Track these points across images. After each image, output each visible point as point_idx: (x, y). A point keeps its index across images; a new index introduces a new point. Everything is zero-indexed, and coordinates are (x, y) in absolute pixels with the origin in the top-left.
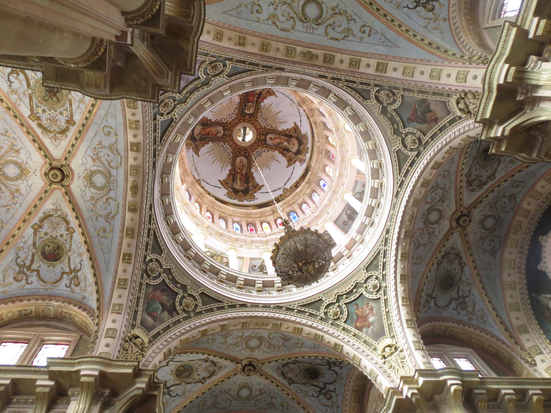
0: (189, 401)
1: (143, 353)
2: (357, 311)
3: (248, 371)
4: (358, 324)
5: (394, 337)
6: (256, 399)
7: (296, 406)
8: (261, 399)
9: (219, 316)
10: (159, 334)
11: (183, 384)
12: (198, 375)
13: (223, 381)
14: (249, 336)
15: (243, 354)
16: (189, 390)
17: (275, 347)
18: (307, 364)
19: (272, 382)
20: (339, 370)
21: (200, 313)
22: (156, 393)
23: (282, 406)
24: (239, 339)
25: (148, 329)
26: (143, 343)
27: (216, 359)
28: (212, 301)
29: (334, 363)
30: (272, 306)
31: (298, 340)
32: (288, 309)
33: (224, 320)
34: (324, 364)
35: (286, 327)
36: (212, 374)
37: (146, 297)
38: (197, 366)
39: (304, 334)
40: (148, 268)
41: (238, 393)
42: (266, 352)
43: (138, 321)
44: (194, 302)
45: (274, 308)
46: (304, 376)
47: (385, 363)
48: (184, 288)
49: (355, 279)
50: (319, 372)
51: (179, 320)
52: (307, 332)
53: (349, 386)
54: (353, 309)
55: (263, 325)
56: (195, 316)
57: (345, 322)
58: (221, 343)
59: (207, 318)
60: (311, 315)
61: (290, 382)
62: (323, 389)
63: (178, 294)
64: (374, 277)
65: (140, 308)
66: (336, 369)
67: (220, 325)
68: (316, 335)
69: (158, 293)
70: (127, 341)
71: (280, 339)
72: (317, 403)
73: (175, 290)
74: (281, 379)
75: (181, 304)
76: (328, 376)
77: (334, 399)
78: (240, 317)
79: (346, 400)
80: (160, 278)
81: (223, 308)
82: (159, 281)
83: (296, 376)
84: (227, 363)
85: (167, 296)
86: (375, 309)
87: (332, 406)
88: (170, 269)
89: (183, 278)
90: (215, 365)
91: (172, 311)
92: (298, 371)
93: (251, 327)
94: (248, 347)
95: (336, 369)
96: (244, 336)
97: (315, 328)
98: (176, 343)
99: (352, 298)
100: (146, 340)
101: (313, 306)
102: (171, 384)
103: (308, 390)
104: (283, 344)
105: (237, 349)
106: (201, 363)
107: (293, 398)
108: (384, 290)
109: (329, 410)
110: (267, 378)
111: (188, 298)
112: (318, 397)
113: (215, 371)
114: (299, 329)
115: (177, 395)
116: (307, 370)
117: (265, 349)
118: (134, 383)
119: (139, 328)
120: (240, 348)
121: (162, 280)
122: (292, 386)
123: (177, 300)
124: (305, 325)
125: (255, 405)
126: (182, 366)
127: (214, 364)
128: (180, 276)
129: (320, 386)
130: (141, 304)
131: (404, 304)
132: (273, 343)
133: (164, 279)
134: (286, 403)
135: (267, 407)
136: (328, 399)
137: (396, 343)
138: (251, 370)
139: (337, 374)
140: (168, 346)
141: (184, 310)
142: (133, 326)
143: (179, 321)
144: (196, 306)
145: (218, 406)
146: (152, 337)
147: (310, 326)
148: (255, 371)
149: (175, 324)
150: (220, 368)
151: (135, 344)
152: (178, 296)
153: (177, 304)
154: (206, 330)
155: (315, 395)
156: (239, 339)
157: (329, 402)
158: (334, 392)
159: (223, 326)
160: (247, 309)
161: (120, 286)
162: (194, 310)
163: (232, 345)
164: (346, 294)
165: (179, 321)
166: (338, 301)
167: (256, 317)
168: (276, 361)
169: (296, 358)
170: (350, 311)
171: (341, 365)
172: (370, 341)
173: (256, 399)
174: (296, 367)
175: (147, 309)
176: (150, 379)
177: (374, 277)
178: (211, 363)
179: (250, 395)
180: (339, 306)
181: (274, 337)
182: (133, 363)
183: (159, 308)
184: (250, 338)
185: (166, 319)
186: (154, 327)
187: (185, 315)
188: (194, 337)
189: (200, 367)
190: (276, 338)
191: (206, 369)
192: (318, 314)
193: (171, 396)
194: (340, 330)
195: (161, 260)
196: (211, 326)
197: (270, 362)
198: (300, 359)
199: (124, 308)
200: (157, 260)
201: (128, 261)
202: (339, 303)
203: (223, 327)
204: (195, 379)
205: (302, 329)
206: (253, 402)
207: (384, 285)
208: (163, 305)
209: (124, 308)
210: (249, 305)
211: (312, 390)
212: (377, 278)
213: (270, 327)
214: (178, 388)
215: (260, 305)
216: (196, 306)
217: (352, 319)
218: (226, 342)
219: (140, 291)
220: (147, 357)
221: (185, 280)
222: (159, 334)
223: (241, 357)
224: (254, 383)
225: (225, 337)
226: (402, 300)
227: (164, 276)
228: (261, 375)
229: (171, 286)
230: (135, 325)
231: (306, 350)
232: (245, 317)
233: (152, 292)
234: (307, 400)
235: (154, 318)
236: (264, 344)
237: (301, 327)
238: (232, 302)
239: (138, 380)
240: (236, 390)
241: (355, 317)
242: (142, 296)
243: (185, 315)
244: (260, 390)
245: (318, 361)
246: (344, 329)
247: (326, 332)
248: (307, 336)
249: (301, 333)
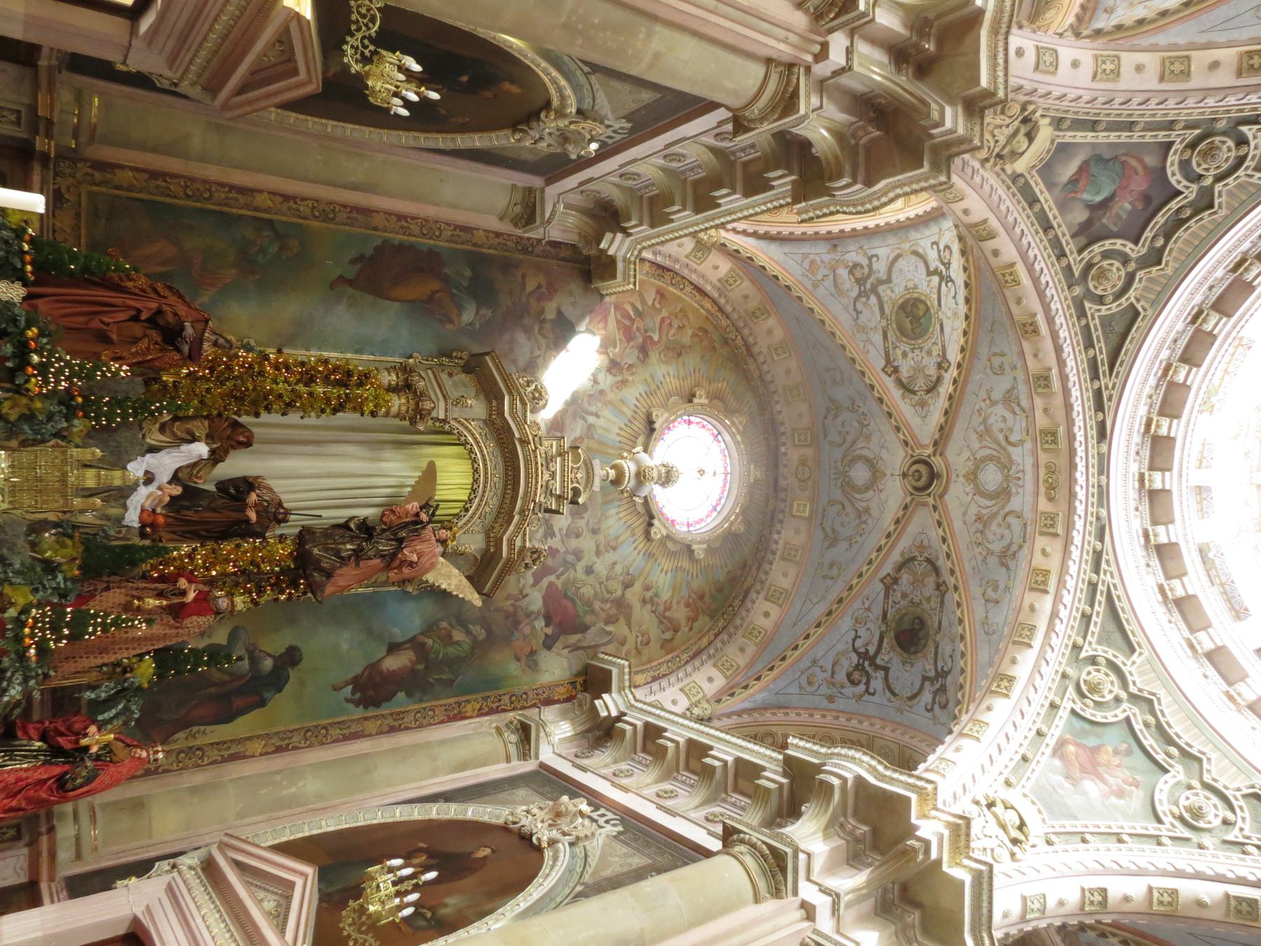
0: (845, 342)
1: (992, 160)
2: (1110, 749)
3: (917, 471)
4: (1071, 748)
5: (1049, 843)
6: (847, 504)
7: (833, 596)
8: (847, 515)
9: (1075, 364)
10: (1032, 201)
11: (884, 323)
12: (905, 355)
13: (890, 415)
14: (1011, 461)
15: (957, 457)
16: (869, 340)
17: (982, 532)
18: (936, 619)
19: (889, 536)
20: (922, 704)
21: (1082, 313)
22: (926, 167)
23: (831, 565)
24: (1001, 437)
25: (1047, 169)
26: (1016, 155)
27: (946, 388)
28: (1116, 340)
29: (943, 689)
30: (1103, 512)
31: (1007, 588)
32: (1098, 556)
33: (1064, 378)
34: (940, 665)
35: (1048, 549)
36: (907, 388)
37: (1132, 149)
38: (927, 346)
39: (1029, 598)
40: (1217, 139)
41: (860, 457)
42: (965, 514)
43: (1069, 137)
44: (1110, 291)
45: (1098, 518)
46: (905, 614)
47: (977, 803)
48: (1154, 257)
49: (1214, 756)
50: (915, 653)
51: (1064, 255)
52: (1037, 606)
53: (883, 728)
54: (1114, 739)
55: (1051, 487)
56: (1073, 298)
57: (1073, 712)
58: (989, 391)
59: (1067, 334)
60: (1086, 618)
61: (888, 580)
62: (873, 663)
63: (1136, 242)
64: (1230, 816)
65: (1102, 137)
66: (927, 697)
67: (1050, 369)
68: (1033, 628)
69: (1139, 184)
70: (1024, 109)
71: (1005, 543)
72: (841, 647)
73: (1148, 234)
74: (896, 557)
75: (1106, 255)
76: (906, 675)
77: (849, 690)
78: (1070, 422)
79: (849, 720)
80: (1185, 183)
81: (1095, 376)
82: (1175, 178)
83: (904, 596)
84: (936, 417)
85: (1130, 214)
86: (1122, 802)
87: (833, 684)
88: (1212, 206)
89: (1181, 251)
90: (928, 391)
91: (1088, 234)
92: (917, 600)
93: (1043, 458)
94: (979, 464)
95: (927, 697)
96: (1010, 449)
97: (1051, 627)
98: (1009, 252)
99: (1149, 741)
100: (1020, 166)
101: (1112, 627)
102: (882, 294)
103: (870, 625)
104: (990, 552)
105: (974, 436)
106: (935, 353)
107: (851, 588)
108: (1188, 840)
109: (824, 675)
110: (897, 522)
111: (1123, 273)
112: (855, 650)
113: (914, 392)
114: (1045, 583)
115: (858, 313)
116: (922, 622)
117: (973, 510)
118: (952, 103)
119: (1052, 142)
120: (976, 445)
121: (1180, 187)
122: (880, 587)
123: (1118, 244)
124: (1058, 599)
125: (831, 503)
126: (928, 309)
127: (932, 388)
128: (1187, 242)
129: (880, 656)
130: (1113, 137)
131: (1156, 894)
132: (994, 527)
133: (1180, 193)
134: (839, 575)
135: (829, 531)
136: (849, 676)
137: (1033, 846)
138: (919, 480)
139: (911, 698)
140: (1001, 230)
141: (1089, 266)
142: (1058, 123)
143: (1061, 255)
144: (1100, 300)
145: (831, 417)
146: (1027, 183)
147: (1054, 614)
148: (915, 488)
149: (1056, 244)
150: (923, 404)
151: (1016, 132)
152: (1130, 245)
153: (1107, 244)
154: (1036, 331)
155: (859, 643)
156: (1001, 437)
157: (841, 677)
158: (867, 691)
159: (1047, 378)
160: (1093, 442)
161: (1167, 64)
162: (1089, 295)
163: (985, 421)
164: (1159, 726)
165: (1061, 255)
166: (1134, 698)
167: (1073, 466)
168: (944, 540)
169: (956, 588)
170: (1107, 730)
171: (936, 707)
172: (1028, 773)
173: (847, 504)
174: (927, 594)
175: (1099, 159)
176: (961, 141)
177: (1230, 816)
178: (934, 379)
179: (854, 488)
180: (1117, 700)
181: (1009, 526)
182: (1001, 87)
183: (1098, 193)
184: (1005, 465)
185: (1069, 217)
186: (1050, 186)
188: (1019, 301)
189: (924, 354)
190: (1006, 532)
191: (919, 369)
192: (1089, 638)
193: (856, 300)
194: (1051, 696)
195: (1241, 172)
196: (1048, 343)
197: (939, 524)
198: (952, 597)
199: (1110, 86)
200: (1241, 160)
201: (1245, 65)
202: (1128, 701)
203: (1043, 380)
204: (894, 348)
205: (1046, 592)
206: (838, 495)
207: (1206, 840)
208: (1105, 204)
209: (1110, 86)
210: (1104, 448)
211: (869, 637)
212: (1225, 822)
213: (1044, 505)
214: (873, 313)
215: (1104, 478)
216: (1100, 300)
217: (1083, 733)
218: (994, 403)
219: (1150, 127)
220: (981, 171)
221: (1176, 259)
222: (1032, 201)
223: (950, 452)
224: (883, 496)
225: (1009, 398)
226: (1166, 890)
227: (1191, 192)
228: (906, 507)
229: (1160, 219)
230: (1060, 130)
231: (979, 612)
232: (1071, 437)
233: (1145, 167)
234: (846, 624)
235: (1074, 181)
236: (989, 503)
237: (1052, 587)
238: (1110, 399)
239: (960, 109)
240: (866, 453)
241: (1091, 742)
242: (1136, 137)
244: (867, 510)
245: (946, 648)
246: (1054, 706)
247: (1042, 656)
248: (1026, 604)
249: (1032, 589)
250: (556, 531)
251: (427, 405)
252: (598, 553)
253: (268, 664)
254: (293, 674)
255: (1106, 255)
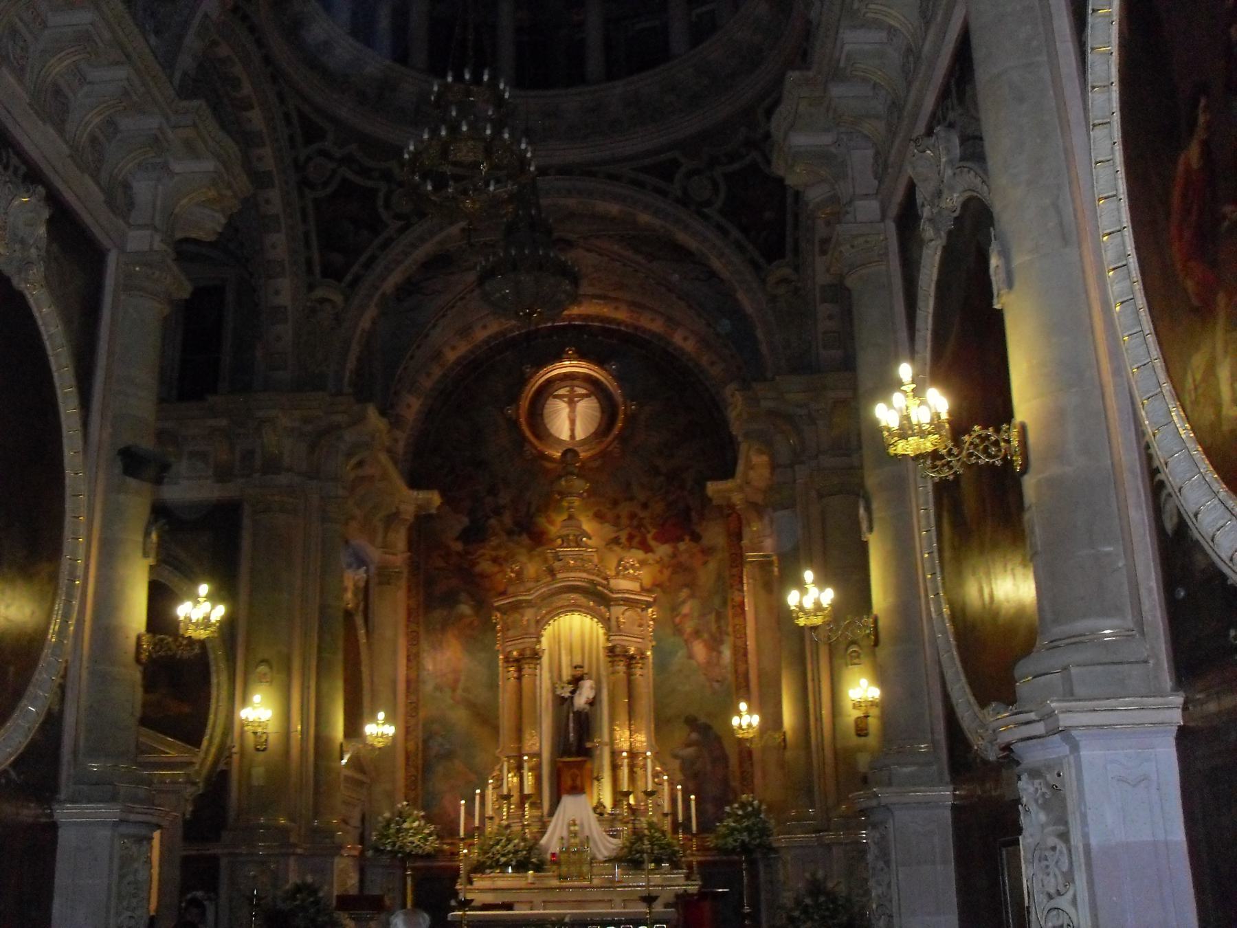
73: (370, 184)
75: (387, 206)
100: (338, 299)
142: (311, 287)
153: (381, 210)
187: (400, 223)
243: (400, 223)
250: (614, 535)
251: (528, 653)
252: (631, 499)
253: (694, 736)
254: (703, 719)
255: (387, 206)
